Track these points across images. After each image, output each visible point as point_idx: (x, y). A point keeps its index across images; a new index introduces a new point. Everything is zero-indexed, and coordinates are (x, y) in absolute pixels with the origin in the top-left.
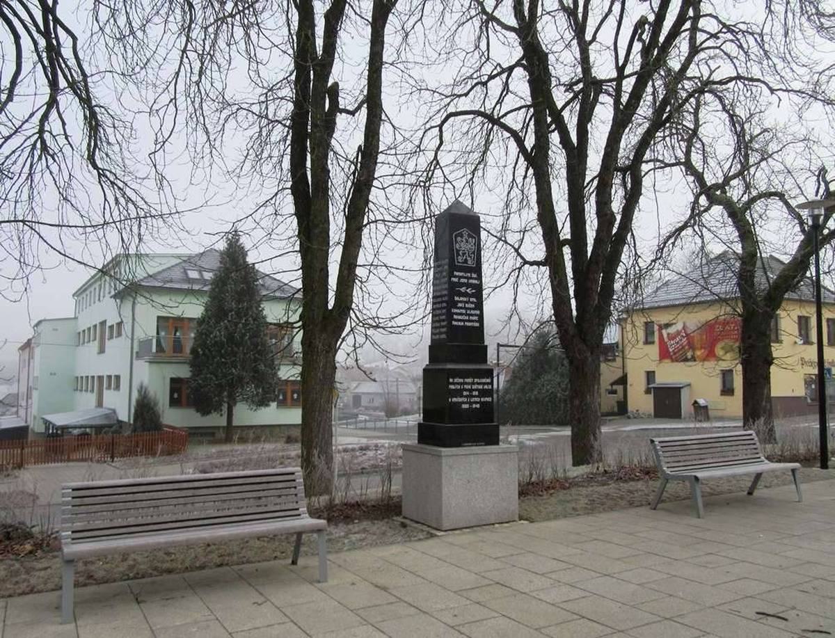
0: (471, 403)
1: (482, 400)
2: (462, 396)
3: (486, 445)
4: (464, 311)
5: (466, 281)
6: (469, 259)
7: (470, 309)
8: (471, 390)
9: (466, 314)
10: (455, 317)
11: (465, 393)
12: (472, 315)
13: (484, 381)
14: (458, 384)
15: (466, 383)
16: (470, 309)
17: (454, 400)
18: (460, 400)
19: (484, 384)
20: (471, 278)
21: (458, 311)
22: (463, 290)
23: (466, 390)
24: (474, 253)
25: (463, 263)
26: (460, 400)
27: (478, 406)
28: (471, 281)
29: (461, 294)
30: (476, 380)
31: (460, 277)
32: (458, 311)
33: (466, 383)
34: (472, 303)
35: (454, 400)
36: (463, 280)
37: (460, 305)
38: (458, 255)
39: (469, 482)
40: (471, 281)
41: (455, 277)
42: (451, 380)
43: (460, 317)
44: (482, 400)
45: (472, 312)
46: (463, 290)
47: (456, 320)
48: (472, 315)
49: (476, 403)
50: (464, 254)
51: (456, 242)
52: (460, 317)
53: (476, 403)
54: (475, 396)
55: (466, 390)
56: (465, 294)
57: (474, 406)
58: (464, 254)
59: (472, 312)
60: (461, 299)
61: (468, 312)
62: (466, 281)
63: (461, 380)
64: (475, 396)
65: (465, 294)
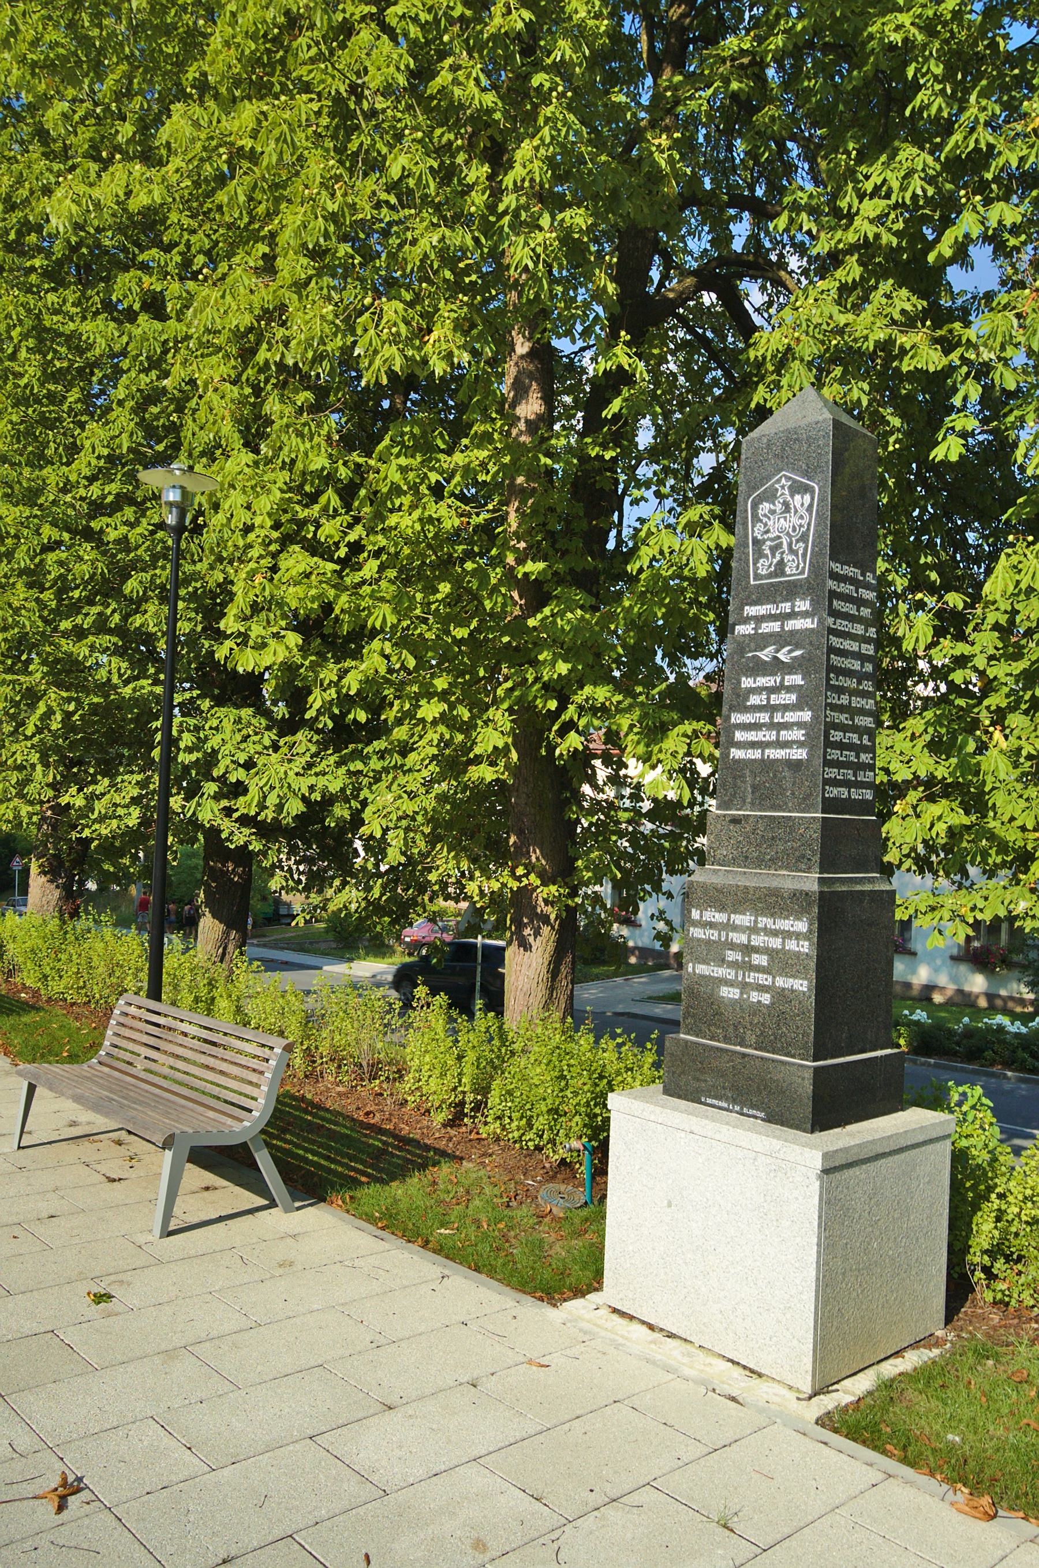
0: (744, 986)
1: (780, 982)
2: (722, 961)
3: (769, 1120)
4: (764, 717)
5: (775, 626)
6: (788, 557)
7: (786, 708)
8: (748, 949)
9: (772, 726)
10: (739, 736)
11: (732, 956)
12: (787, 726)
13: (785, 924)
14: (711, 925)
15: (735, 928)
16: (786, 708)
17: (702, 969)
18: (720, 972)
19: (787, 935)
20: (793, 615)
21: (747, 718)
22: (765, 655)
23: (733, 946)
24: (804, 538)
25: (770, 576)
26: (720, 972)
27: (766, 998)
28: (792, 625)
29: (759, 668)
30: (764, 921)
31: (759, 620)
32: (747, 718)
33: (735, 928)
34: (789, 689)
35: (702, 969)
36: (768, 627)
37: (754, 700)
38: (759, 554)
39: (670, 1205)
40: (792, 625)
41: (746, 620)
42: (695, 914)
43: (752, 736)
44: (780, 982)
45: (791, 717)
46: (765, 655)
47: (740, 745)
48: (787, 726)
49: (762, 989)
50: (774, 549)
51: (756, 519)
52: (752, 736)
53: (762, 989)
54: (758, 969)
55: (733, 946)
56: (776, 666)
57: (755, 996)
58: (774, 549)
59: (791, 717)
60: (763, 681)
61: (778, 718)
62: (775, 626)
63: (720, 917)
64: (758, 969)
65: (776, 666)
